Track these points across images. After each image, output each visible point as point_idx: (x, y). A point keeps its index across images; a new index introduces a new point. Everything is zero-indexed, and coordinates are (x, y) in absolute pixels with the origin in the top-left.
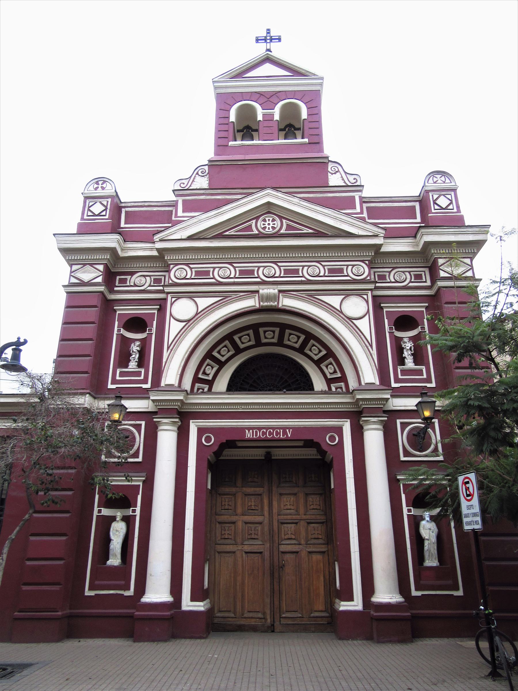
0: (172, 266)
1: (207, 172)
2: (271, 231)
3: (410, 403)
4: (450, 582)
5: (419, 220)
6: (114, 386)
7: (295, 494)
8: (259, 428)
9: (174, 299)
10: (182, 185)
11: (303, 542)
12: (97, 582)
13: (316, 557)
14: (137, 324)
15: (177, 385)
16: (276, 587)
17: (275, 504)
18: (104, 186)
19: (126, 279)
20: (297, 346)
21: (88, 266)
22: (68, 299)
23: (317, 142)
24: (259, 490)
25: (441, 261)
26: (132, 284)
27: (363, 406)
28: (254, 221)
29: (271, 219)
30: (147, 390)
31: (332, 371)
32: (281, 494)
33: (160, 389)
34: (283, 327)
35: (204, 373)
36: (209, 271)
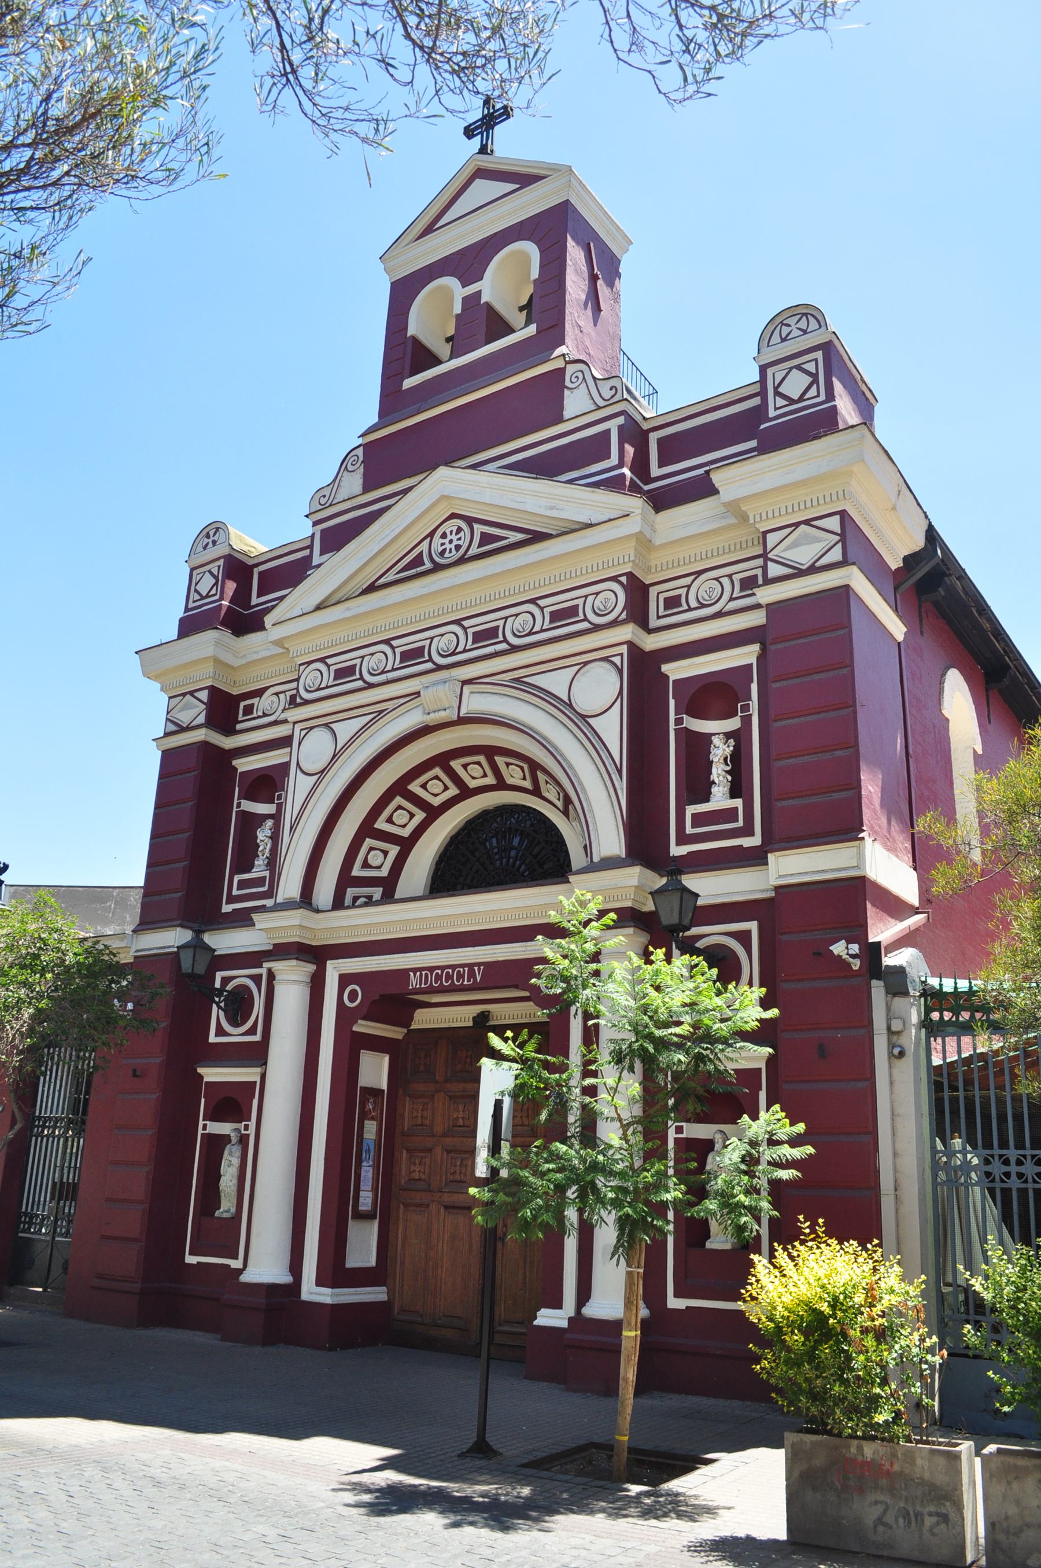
1: (361, 459)
2: (453, 556)
8: (431, 969)
9: (303, 733)
19: (253, 705)
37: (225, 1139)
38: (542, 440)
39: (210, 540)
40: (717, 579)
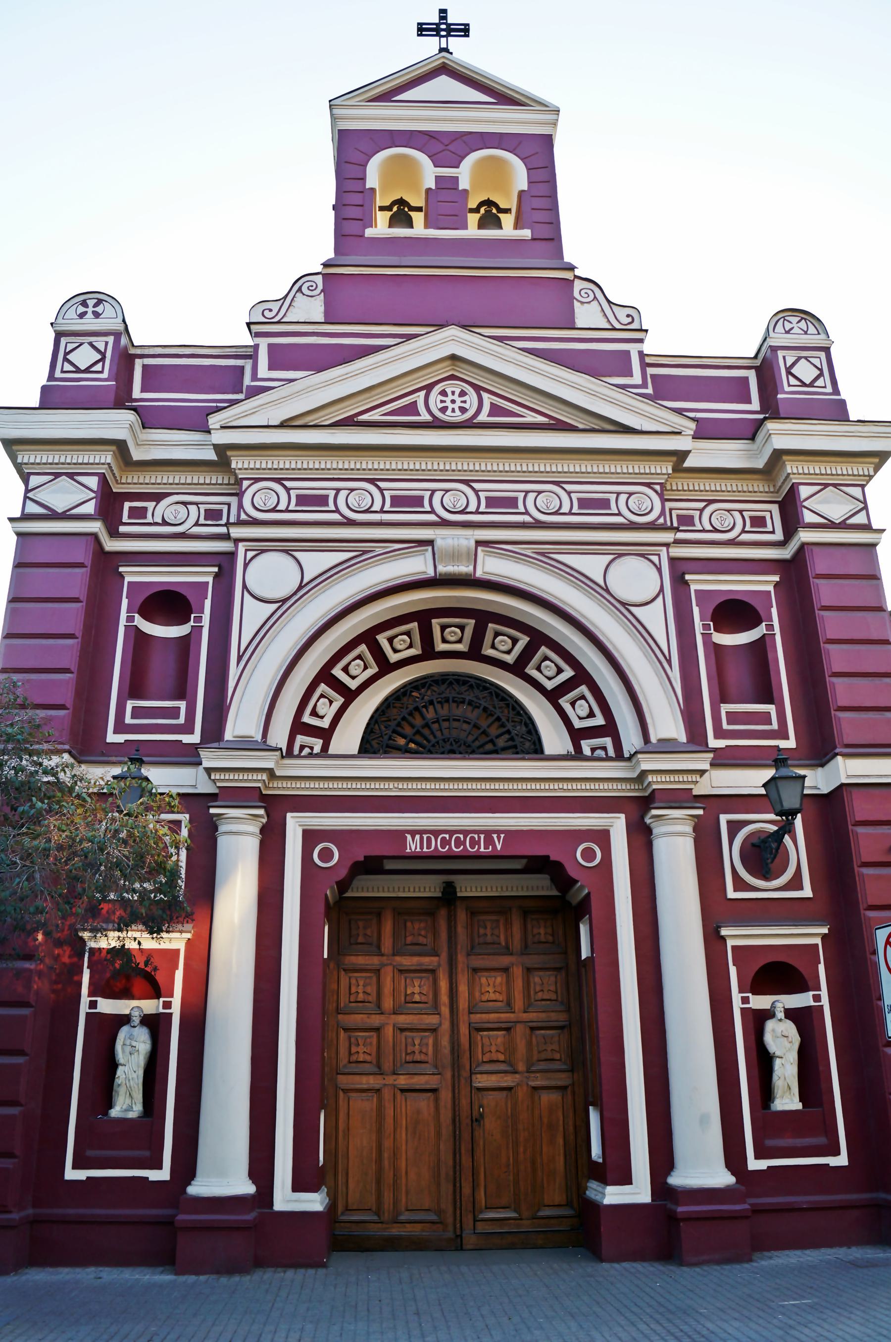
0: (246, 483)
1: (320, 287)
3: (752, 780)
4: (822, 1140)
5: (755, 405)
6: (121, 738)
7: (506, 970)
8: (436, 833)
9: (250, 554)
10: (267, 313)
11: (521, 1067)
12: (90, 1153)
13: (547, 1098)
14: (169, 604)
15: (259, 737)
16: (466, 1161)
17: (463, 988)
18: (99, 309)
19: (146, 509)
20: (510, 659)
21: (64, 477)
22: (20, 549)
23: (550, 237)
24: (428, 961)
25: (804, 492)
26: (160, 521)
27: (654, 787)
28: (422, 394)
29: (458, 391)
30: (195, 747)
31: (584, 712)
32: (475, 970)
33: (222, 745)
34: (483, 618)
35: (314, 713)
36: (327, 496)
37: (124, 1020)
38: (555, 339)
39: (90, 310)
40: (728, 511)
